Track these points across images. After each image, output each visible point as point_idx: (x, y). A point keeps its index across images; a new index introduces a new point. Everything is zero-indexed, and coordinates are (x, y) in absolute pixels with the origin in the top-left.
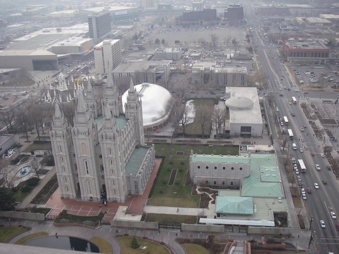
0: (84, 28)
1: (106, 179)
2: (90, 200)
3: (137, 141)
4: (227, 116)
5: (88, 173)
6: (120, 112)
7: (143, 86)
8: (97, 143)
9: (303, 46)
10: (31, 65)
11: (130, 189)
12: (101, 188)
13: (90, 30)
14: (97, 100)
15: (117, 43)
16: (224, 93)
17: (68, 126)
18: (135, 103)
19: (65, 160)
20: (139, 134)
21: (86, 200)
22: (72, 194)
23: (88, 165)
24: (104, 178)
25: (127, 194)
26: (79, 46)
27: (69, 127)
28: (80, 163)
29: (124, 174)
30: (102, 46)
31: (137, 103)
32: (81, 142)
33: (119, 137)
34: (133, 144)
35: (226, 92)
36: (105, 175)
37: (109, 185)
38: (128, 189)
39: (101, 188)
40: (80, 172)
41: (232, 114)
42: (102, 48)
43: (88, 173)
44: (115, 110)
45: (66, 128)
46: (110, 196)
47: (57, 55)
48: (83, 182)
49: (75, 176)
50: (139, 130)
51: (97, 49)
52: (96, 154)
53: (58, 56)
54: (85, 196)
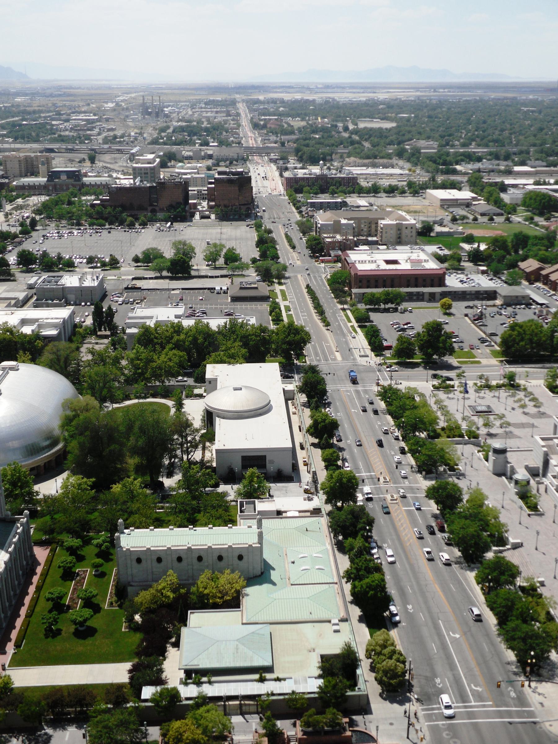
9: (388, 262)
35: (208, 376)
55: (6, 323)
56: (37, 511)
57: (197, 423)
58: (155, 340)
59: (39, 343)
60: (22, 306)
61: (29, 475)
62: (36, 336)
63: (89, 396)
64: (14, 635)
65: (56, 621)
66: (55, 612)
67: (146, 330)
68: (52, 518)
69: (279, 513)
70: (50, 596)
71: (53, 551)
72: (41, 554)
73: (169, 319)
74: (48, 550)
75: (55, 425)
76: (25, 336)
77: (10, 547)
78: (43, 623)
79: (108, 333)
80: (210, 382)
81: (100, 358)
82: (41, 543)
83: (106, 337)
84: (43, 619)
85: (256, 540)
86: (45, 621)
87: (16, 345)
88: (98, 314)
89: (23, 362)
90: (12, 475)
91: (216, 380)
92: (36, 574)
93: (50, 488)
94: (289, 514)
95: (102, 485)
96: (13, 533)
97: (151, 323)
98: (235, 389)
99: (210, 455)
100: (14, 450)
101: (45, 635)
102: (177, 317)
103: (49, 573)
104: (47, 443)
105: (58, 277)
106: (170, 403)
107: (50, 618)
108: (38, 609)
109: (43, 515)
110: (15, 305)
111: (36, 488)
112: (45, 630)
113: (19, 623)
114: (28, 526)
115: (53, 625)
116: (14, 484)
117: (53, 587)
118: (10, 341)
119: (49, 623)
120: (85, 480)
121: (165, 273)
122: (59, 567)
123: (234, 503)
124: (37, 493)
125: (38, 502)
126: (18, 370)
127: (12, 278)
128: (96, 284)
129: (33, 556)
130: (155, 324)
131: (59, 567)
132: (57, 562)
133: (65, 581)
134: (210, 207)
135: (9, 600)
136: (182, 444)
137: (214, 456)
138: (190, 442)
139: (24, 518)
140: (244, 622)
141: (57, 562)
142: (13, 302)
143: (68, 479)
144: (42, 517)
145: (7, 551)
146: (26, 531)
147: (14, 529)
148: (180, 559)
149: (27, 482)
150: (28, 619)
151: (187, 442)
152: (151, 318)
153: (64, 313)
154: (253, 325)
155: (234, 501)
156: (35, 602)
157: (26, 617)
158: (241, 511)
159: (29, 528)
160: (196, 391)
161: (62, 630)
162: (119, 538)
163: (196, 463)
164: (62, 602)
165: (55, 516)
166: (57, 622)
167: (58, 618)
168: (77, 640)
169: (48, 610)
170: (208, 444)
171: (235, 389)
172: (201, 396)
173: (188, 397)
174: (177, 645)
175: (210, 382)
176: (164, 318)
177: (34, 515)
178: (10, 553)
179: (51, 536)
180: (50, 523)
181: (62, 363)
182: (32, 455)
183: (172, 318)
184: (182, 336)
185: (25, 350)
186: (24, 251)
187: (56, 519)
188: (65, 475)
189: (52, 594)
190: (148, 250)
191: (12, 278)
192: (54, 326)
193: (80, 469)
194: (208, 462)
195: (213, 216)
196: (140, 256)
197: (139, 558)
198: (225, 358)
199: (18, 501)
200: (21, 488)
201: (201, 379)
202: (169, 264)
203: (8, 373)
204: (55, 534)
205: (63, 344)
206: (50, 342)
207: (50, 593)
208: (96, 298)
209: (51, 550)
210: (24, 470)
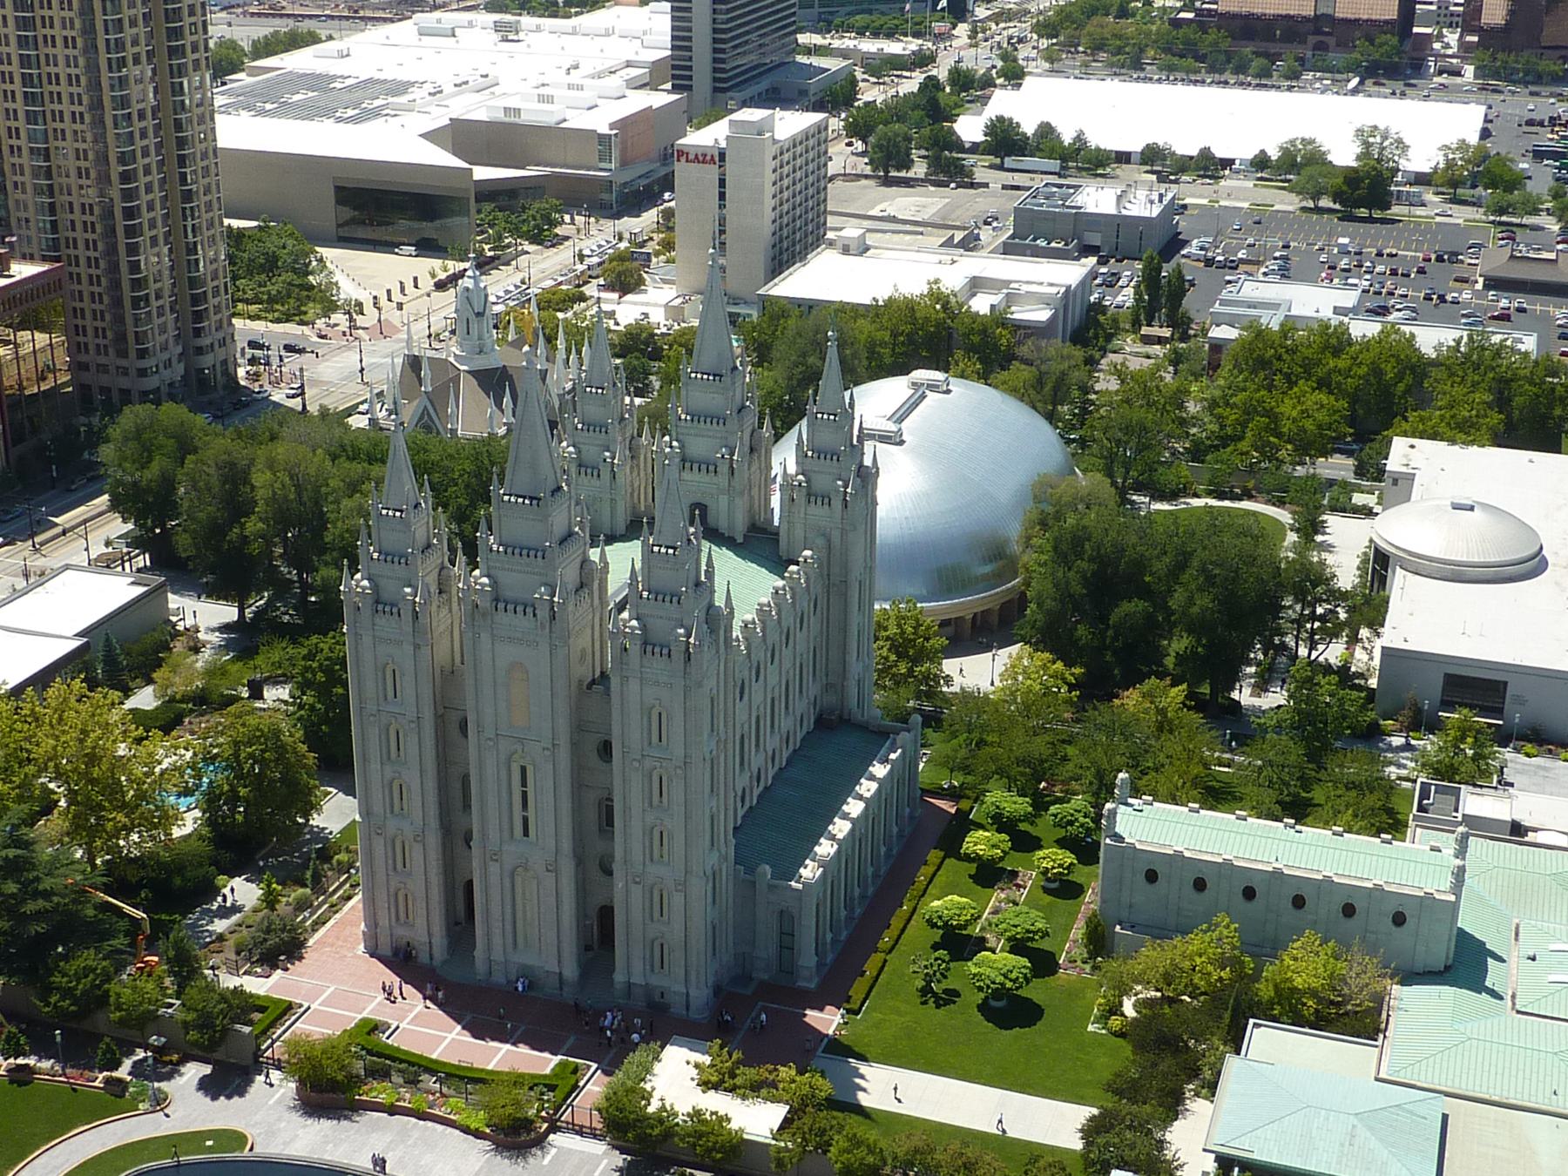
0: (645, 33)
1: (619, 885)
3: (828, 687)
4: (1370, 606)
5: (526, 834)
7: (915, 385)
8: (598, 674)
10: (327, 212)
13: (673, 48)
15: (806, 135)
16: (1380, 474)
18: (845, 474)
23: (530, 790)
26: (604, 129)
30: (723, 144)
34: (801, 706)
35: (1393, 464)
41: (1408, 596)
42: (722, 156)
43: (526, 834)
44: (723, 500)
48: (494, 879)
50: (844, 630)
51: (691, 157)
52: (579, 728)
53: (482, 173)
55: (937, 281)
57: (1346, 572)
58: (1277, 365)
59: (1004, 338)
62: (999, 318)
63: (1099, 476)
67: (1259, 333)
69: (1517, 830)
73: (1320, 315)
75: (1014, 531)
79: (1166, 332)
80: (1395, 482)
81: (1139, 387)
83: (1160, 341)
85: (1446, 882)
88: (1151, 280)
91: (1410, 478)
93: (976, 673)
94: (1540, 837)
95: (1096, 688)
97: (1273, 322)
98: (1456, 507)
99: (1367, 659)
102: (1336, 310)
104: (987, 569)
105: (1069, 187)
106: (1284, 516)
111: (950, 666)
120: (1059, 665)
121: (1325, 202)
123: (1408, 785)
124: (948, 680)
125: (947, 700)
128: (1156, 211)
130: (1282, 325)
134: (1464, 46)
136: (1299, 623)
137: (1377, 662)
138: (1322, 618)
140: (1382, 1075)
142: (959, 236)
143: (1020, 658)
148: (1249, 893)
151: (1313, 617)
152: (1275, 306)
153: (1070, 273)
154: (1526, 354)
155: (1407, 779)
158: (1421, 809)
160: (1358, 499)
162: (1113, 813)
163: (1327, 669)
170: (1364, 633)
171: (1456, 507)
172: (1368, 513)
173: (1334, 509)
174: (1211, 1088)
175: (1395, 482)
176: (1308, 312)
181: (1048, 388)
182: (949, 590)
183: (1327, 313)
184: (1342, 363)
185: (971, 349)
186: (1000, 119)
188: (1015, 649)
190: (1292, 142)
192: (1045, 301)
193: (1052, 639)
194: (1361, 675)
195: (1469, 71)
196: (1274, 154)
197: (1153, 870)
198: (1442, 428)
200: (916, 661)
201: (1371, 470)
202: (1340, 180)
203: (923, 397)
205: (1056, 346)
206: (1027, 336)
208: (1154, 246)
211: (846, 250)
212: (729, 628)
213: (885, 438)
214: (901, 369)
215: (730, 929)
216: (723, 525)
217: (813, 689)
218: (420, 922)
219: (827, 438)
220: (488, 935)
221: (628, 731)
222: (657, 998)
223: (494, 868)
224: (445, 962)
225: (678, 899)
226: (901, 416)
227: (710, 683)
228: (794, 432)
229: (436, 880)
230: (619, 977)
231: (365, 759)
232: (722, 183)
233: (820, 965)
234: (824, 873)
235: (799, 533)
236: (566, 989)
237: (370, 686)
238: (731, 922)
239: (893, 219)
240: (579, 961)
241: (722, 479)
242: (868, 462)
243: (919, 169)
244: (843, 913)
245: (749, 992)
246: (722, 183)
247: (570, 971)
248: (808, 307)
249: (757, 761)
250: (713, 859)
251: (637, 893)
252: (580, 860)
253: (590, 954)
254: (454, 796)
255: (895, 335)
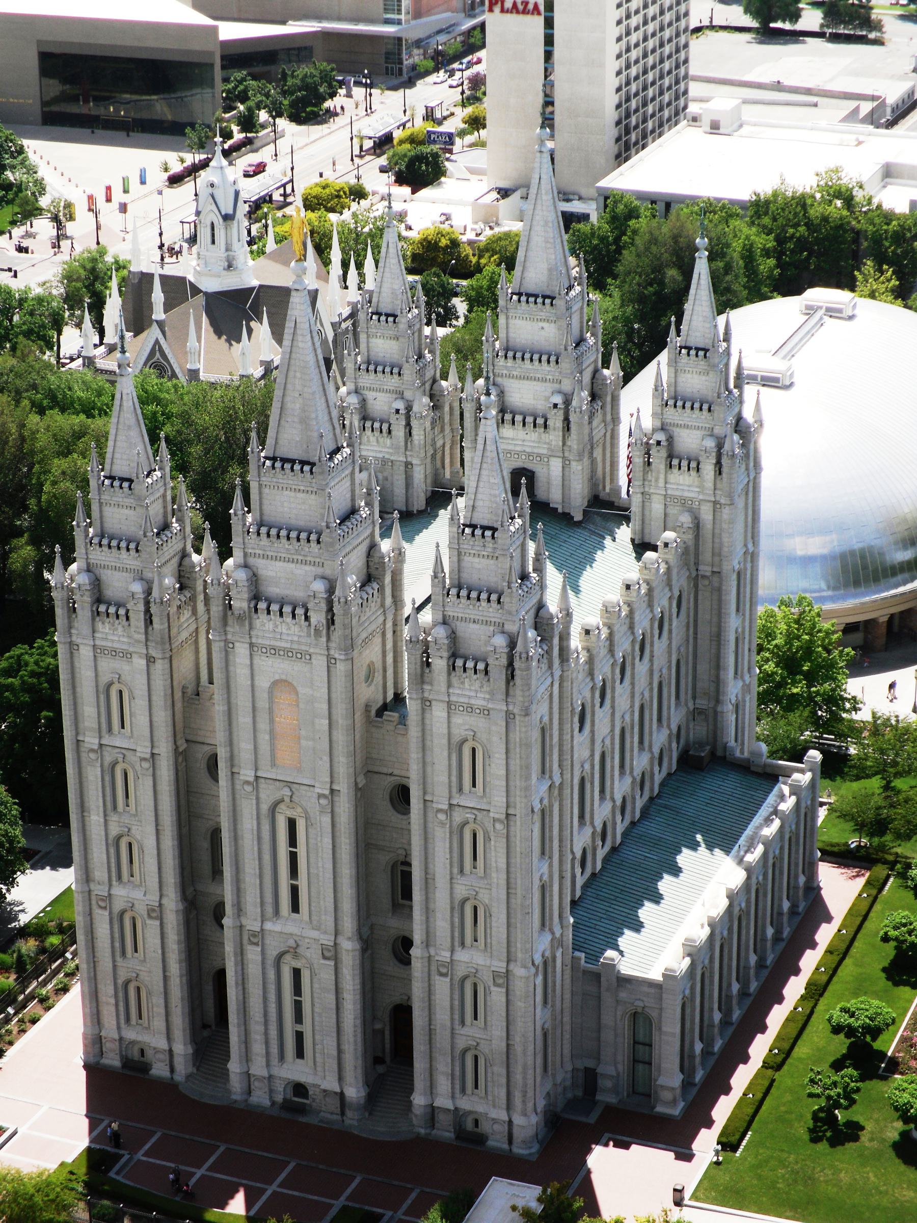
2: (287, 1106)
3: (696, 714)
5: (295, 908)
6: (594, 481)
7: (810, 310)
8: (390, 696)
11: (590, 1064)
12: (378, 1026)
14: (434, 381)
17: (190, 549)
19: (142, 791)
20: (717, 665)
21: (260, 1098)
22: (163, 1039)
23: (301, 850)
24: (406, 961)
25: (570, 1095)
27: (198, 551)
28: (248, 824)
29: (557, 943)
31: (729, 430)
32: (271, 669)
33: (550, 667)
34: (659, 738)
36: (418, 937)
37: (442, 1016)
38: (580, 1065)
39: (382, 1032)
40: (238, 891)
43: (295, 908)
44: (556, 465)
45: (176, 560)
46: (435, 1089)
47: (215, 29)
49: (201, 913)
50: (718, 638)
53: (232, 31)
54: (257, 1066)
55: (837, 171)
56: (846, 757)
60: (891, 124)
61: (841, 643)
64: (723, 1110)
65: (849, 1097)
66: (850, 1071)
68: (887, 787)
70: (845, 1019)
71: (875, 887)
72: (839, 888)
74: (861, 881)
76: (888, 217)
77: (749, 849)
78: (811, 1095)
82: (842, 857)
84: (812, 1081)
86: (818, 1091)
87: (856, 241)
89: (872, 295)
90: (790, 637)
92: (813, 945)
96: (764, 811)
100: (807, 561)
101: (811, 1131)
103: (853, 950)
107: (835, 1084)
108: (802, 1050)
109: (862, 774)
110: (872, 119)
111: (854, 686)
112: (815, 1116)
113: (742, 1078)
114: (813, 799)
115: (838, 1106)
116: (790, 663)
117: (856, 995)
118: (841, 227)
119: (829, 1098)
122: (886, 939)
125: (854, 730)
126: (851, 318)
127: (872, 36)
129: (813, 891)
131: (886, 939)
132: (882, 921)
133: (896, 984)
135: (725, 1007)
139: (802, 771)
141: (882, 921)
142: (866, 107)
144: (858, 778)
145: (740, 861)
146: (805, 813)
147: (771, 799)
149: (832, 665)
150: (770, 1072)
156: (799, 1026)
157: (766, 1065)
159: (815, 805)
161: (862, 1128)
164: (877, 1045)
165: (898, 783)
166: (853, 1102)
167: (858, 1090)
168: (903, 1167)
169: (832, 1059)
177: (834, 766)
178: (749, 870)
179: (876, 840)
180: (878, 800)
182: (857, 583)
185: (881, 260)
187: (899, 792)
189: (852, 1015)
191: (872, 36)
199: (795, 717)
200: (811, 677)
204: (888, 837)
207: (844, 1010)
209: (868, 883)
210: (826, 626)
211: (715, 127)
212: (565, 637)
213: (769, 382)
214: (789, 285)
215: (567, 1036)
216: (555, 497)
217: (676, 716)
218: (159, 1023)
219: (696, 381)
220: (246, 1042)
221: (431, 774)
222: (470, 1126)
223: (253, 954)
224: (189, 1077)
225: (497, 996)
226: (787, 348)
227: (541, 710)
228: (650, 371)
229: (175, 969)
230: (419, 1100)
231: (82, 807)
232: (549, 40)
233: (687, 1084)
234: (693, 965)
235: (657, 507)
236: (349, 1113)
237: (89, 711)
238: (567, 1027)
239: (778, 86)
240: (366, 1074)
241: (554, 437)
242: (748, 414)
243: (811, 19)
244: (717, 1016)
245: (592, 1119)
246: (549, 40)
247: (354, 1092)
248: (666, 205)
249: (601, 812)
250: (543, 943)
251: (442, 986)
252: (367, 943)
253: (381, 1069)
254: (200, 854)
255: (781, 240)
